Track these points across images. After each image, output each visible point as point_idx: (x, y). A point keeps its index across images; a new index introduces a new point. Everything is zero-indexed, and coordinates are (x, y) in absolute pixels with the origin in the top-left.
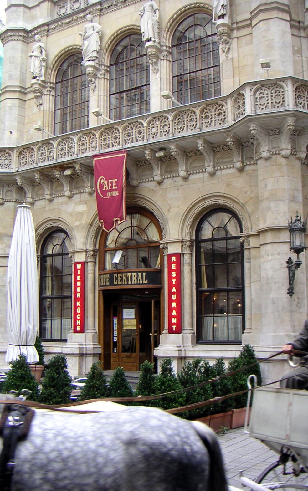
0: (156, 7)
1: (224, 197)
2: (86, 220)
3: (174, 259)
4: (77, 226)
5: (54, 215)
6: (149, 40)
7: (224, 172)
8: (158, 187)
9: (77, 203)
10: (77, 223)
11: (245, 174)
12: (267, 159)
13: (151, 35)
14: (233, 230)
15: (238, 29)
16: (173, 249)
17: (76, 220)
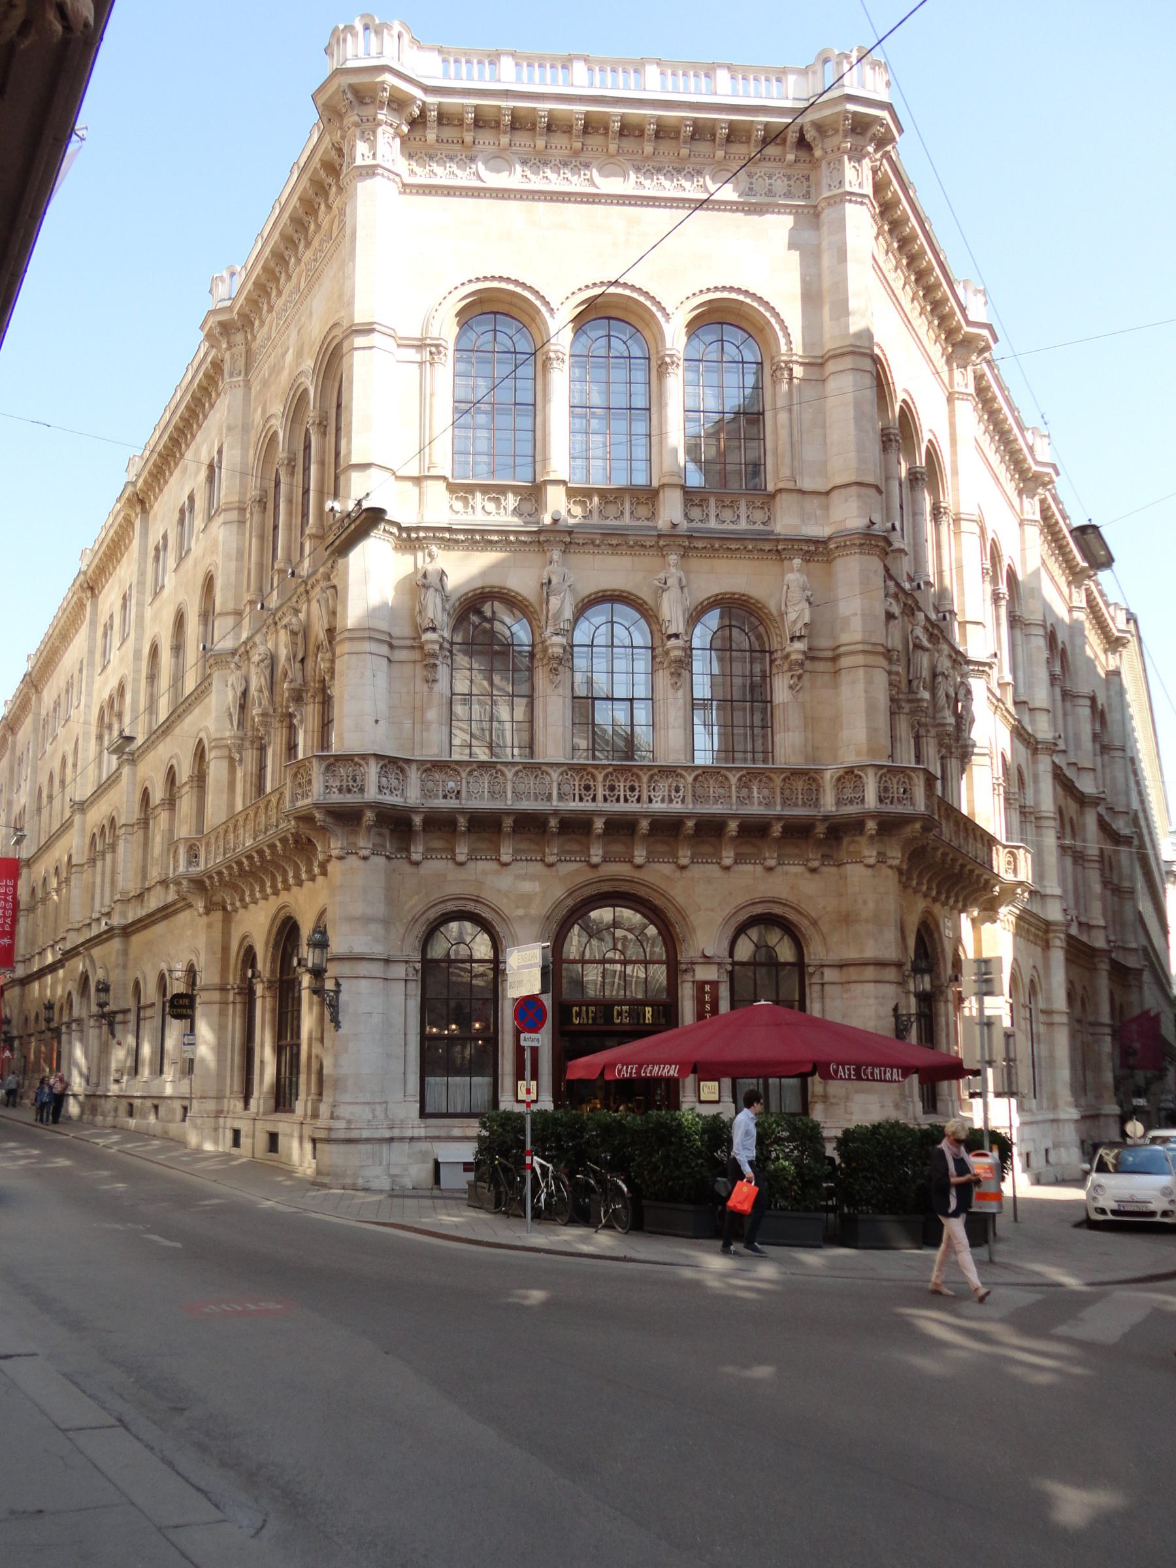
0: (684, 582)
1: (785, 905)
2: (539, 909)
3: (707, 988)
4: (521, 918)
5: (470, 890)
6: (676, 636)
7: (785, 868)
8: (678, 874)
9: (518, 877)
10: (520, 912)
11: (817, 876)
12: (868, 866)
13: (681, 630)
14: (785, 953)
15: (813, 659)
16: (705, 973)
17: (517, 907)
